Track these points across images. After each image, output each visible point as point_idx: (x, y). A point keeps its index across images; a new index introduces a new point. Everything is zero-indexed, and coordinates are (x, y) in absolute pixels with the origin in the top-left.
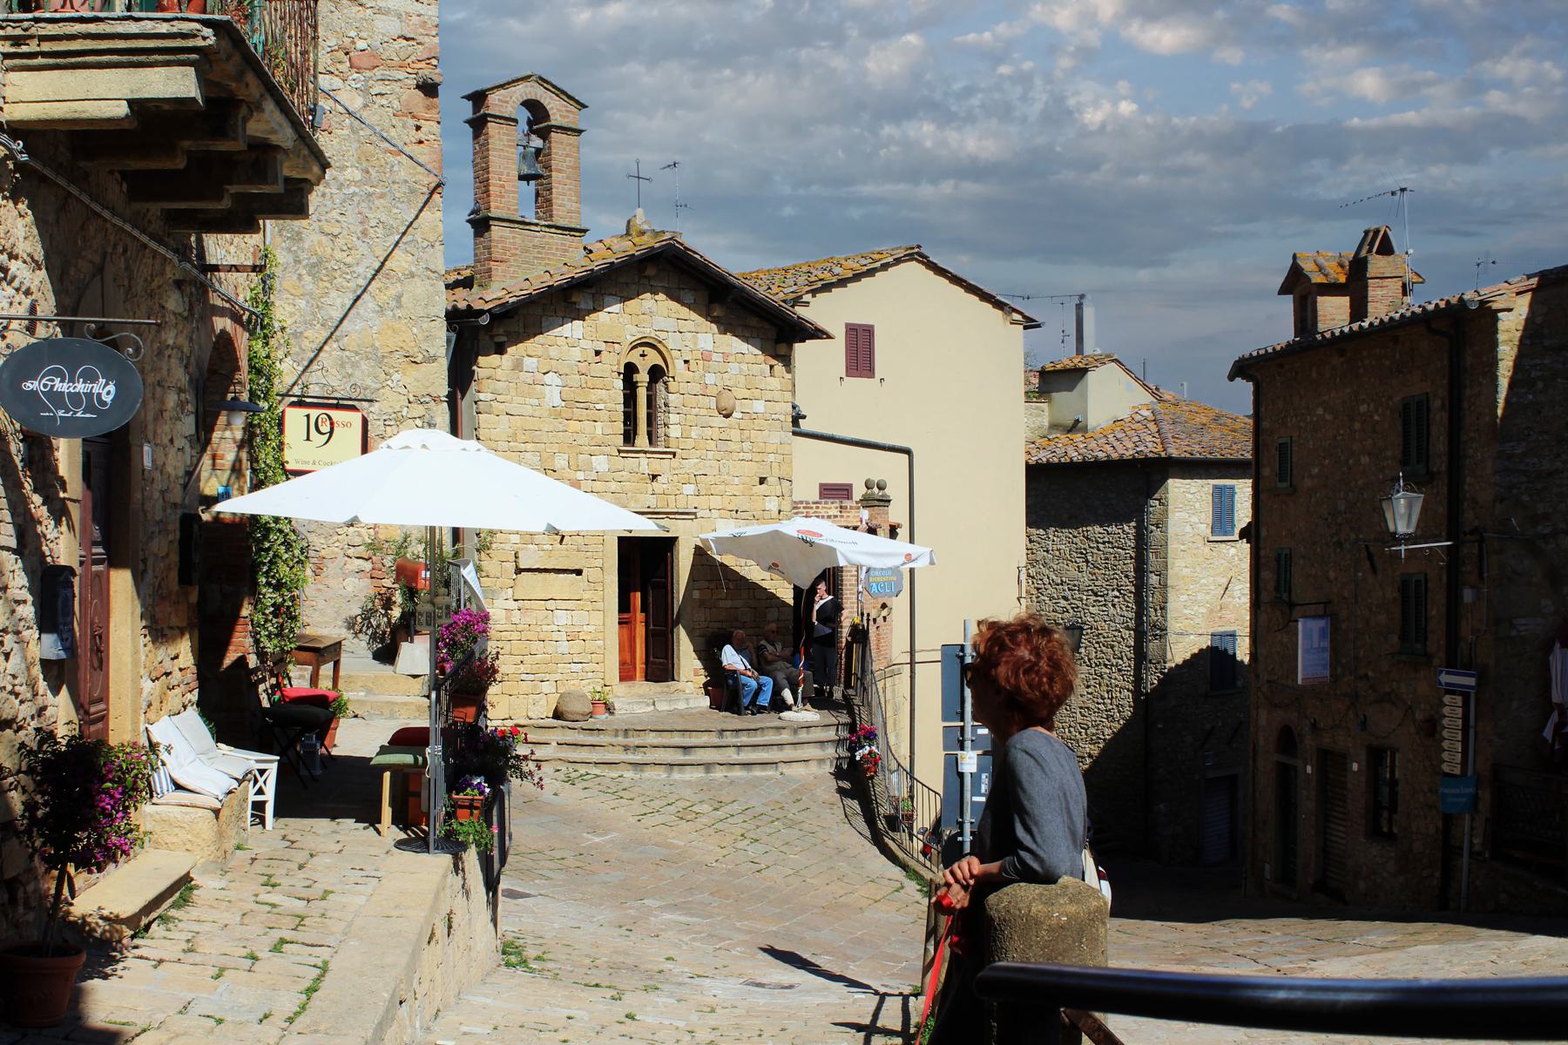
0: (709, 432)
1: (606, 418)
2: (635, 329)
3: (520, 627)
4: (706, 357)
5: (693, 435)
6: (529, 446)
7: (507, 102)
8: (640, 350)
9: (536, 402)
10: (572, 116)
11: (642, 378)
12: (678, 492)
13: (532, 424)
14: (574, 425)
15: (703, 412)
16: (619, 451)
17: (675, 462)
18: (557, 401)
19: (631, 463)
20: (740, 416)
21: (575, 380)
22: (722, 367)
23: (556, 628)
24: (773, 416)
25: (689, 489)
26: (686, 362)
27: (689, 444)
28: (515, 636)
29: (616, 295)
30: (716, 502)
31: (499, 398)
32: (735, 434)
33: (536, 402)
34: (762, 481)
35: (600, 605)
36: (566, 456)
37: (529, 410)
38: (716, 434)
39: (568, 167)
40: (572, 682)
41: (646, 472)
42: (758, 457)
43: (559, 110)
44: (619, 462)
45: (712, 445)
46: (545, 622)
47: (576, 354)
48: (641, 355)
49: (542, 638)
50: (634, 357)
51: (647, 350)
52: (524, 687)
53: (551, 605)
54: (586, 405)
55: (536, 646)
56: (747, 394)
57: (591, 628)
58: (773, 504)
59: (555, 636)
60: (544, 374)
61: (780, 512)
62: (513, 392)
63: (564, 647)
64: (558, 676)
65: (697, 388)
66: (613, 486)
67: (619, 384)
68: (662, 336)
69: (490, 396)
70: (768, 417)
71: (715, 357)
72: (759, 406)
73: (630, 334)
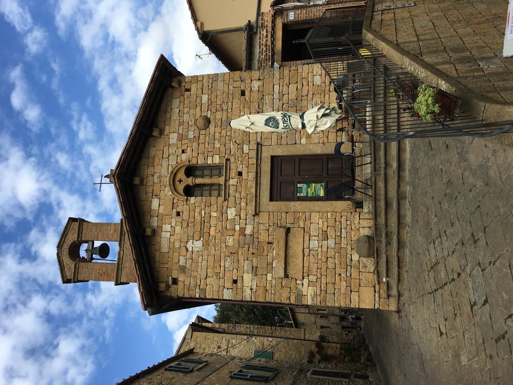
3: (319, 276)
4: (181, 137)
6: (222, 264)
7: (70, 267)
8: (177, 183)
9: (201, 257)
12: (247, 157)
13: (211, 259)
14: (212, 233)
16: (225, 200)
17: (232, 159)
20: (209, 112)
21: (190, 230)
23: (320, 249)
24: (210, 87)
25: (246, 148)
29: (151, 201)
31: (198, 284)
32: (219, 115)
33: (201, 257)
34: (243, 93)
36: (228, 237)
37: (204, 263)
38: (218, 130)
39: (96, 231)
40: (353, 236)
42: (231, 97)
45: (223, 132)
46: (316, 257)
47: (178, 229)
48: (180, 183)
49: (324, 260)
50: (181, 187)
51: (178, 179)
52: (355, 274)
53: (307, 251)
56: (199, 108)
57: (321, 223)
59: (324, 249)
61: (259, 79)
62: (196, 274)
63: (331, 242)
64: (349, 248)
65: (195, 145)
66: (243, 204)
68: (170, 169)
69: (198, 290)
70: (210, 91)
72: (205, 98)
73: (168, 192)
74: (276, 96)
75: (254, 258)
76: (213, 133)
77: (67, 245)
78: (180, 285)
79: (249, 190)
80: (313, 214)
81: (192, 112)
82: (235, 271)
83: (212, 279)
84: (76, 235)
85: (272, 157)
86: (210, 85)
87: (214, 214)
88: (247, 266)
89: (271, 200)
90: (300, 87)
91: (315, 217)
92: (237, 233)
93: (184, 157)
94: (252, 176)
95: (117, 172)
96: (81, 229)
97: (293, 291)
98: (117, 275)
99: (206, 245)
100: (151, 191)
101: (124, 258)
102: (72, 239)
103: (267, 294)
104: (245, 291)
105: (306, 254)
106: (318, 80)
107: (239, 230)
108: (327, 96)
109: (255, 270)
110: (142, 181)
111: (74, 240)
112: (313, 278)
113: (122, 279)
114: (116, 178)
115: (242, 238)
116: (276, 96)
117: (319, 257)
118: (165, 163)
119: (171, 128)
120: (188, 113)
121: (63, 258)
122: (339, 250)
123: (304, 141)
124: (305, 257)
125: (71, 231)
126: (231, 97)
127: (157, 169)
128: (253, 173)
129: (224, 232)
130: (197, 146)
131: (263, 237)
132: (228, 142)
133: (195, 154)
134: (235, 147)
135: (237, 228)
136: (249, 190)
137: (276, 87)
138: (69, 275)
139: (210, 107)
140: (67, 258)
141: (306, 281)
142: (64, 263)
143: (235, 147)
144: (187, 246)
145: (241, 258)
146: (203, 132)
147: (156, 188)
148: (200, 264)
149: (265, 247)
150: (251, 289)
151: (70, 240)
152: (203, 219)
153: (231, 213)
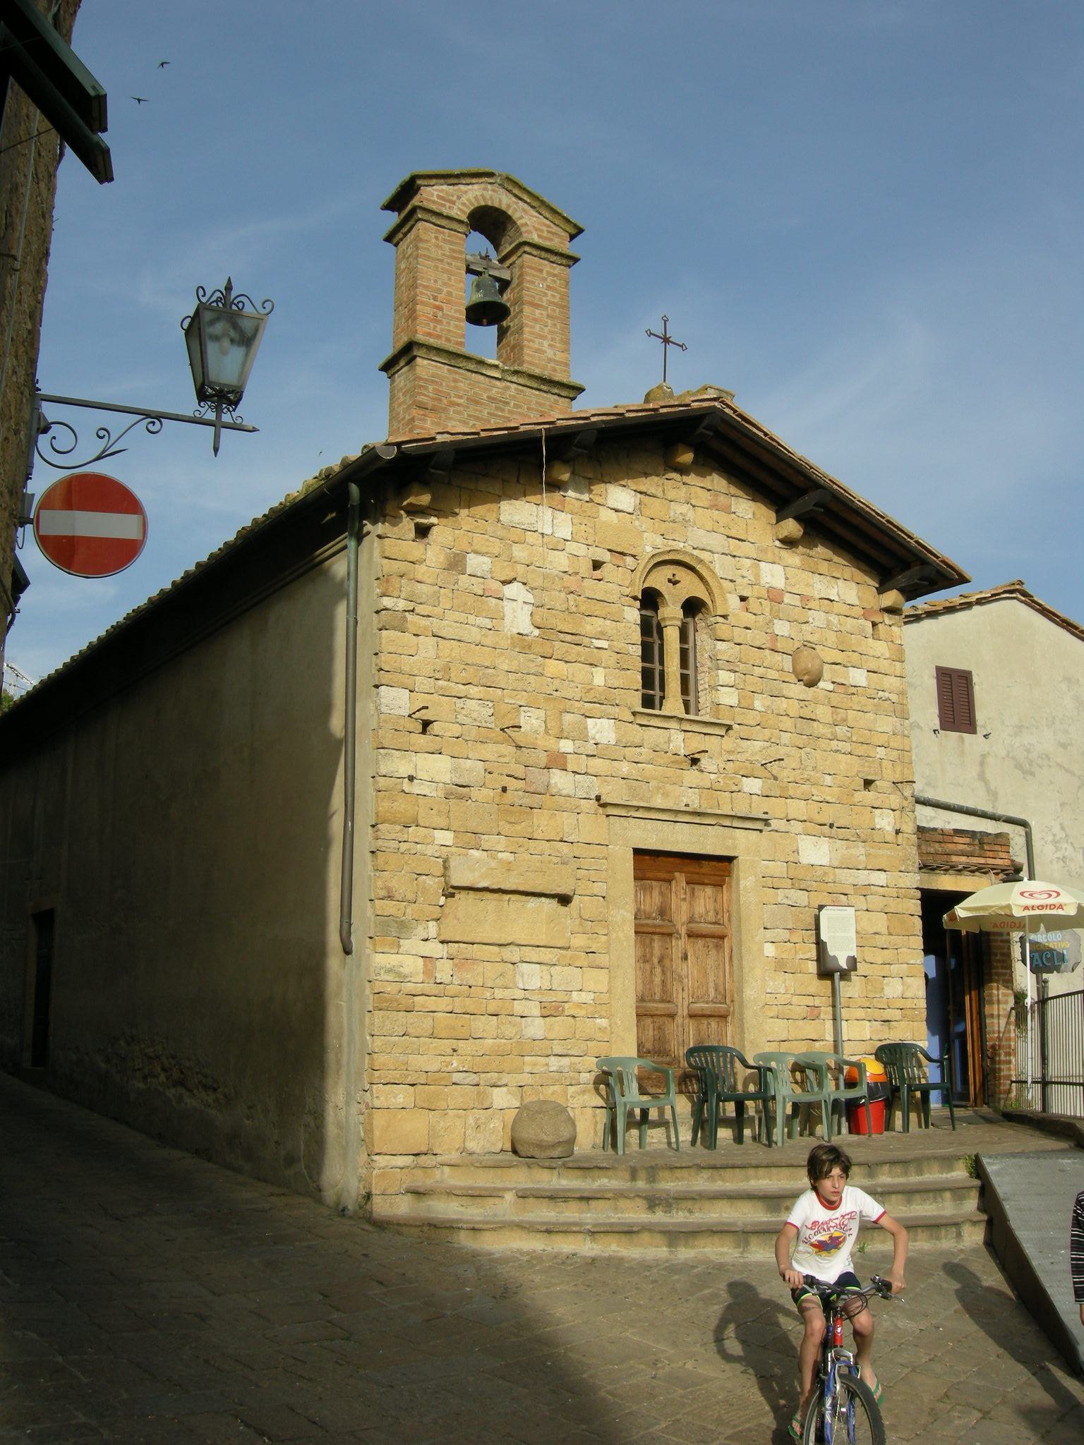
0: (783, 704)
1: (612, 662)
2: (659, 541)
3: (452, 989)
4: (774, 596)
5: (759, 703)
6: (473, 691)
7: (453, 203)
8: (668, 571)
10: (557, 240)
11: (671, 612)
12: (734, 788)
13: (485, 657)
14: (553, 667)
15: (772, 674)
16: (634, 714)
17: (728, 742)
18: (525, 625)
19: (653, 736)
20: (831, 687)
21: (557, 599)
22: (797, 613)
23: (520, 994)
25: (753, 785)
26: (743, 599)
27: (751, 718)
28: (444, 1004)
30: (797, 808)
31: (419, 609)
32: (823, 712)
34: (868, 783)
35: (602, 959)
37: (475, 635)
38: (794, 708)
39: (551, 303)
41: (682, 752)
42: (861, 750)
43: (536, 230)
44: (636, 733)
45: (787, 723)
46: (499, 982)
47: (560, 561)
48: (670, 581)
50: (658, 581)
51: (681, 573)
52: (456, 1096)
53: (513, 954)
54: (576, 638)
55: (482, 1025)
56: (838, 657)
57: (586, 997)
58: (886, 820)
59: (518, 1008)
60: (504, 583)
61: (898, 832)
63: (536, 1027)
64: (525, 1079)
65: (761, 639)
66: (625, 768)
67: (633, 614)
68: (705, 556)
69: (402, 605)
70: (872, 693)
71: (787, 598)
72: (858, 677)
73: (650, 544)
74: (863, 877)
75: (491, 793)
76: (785, 693)
77: (509, 206)
78: (415, 549)
79: (659, 788)
80: (603, 976)
81: (832, 638)
82: (456, 730)
83: (432, 653)
84: (535, 239)
85: (730, 859)
86: (886, 695)
87: (599, 677)
88: (472, 769)
89: (637, 852)
90: (882, 941)
91: (598, 980)
92: (550, 743)
93: (734, 601)
94: (693, 800)
95: (727, 410)
96: (554, 258)
97: (409, 911)
98: (439, 351)
99: (521, 643)
100: (652, 490)
101: (482, 378)
102: (526, 224)
103: (398, 828)
104: (403, 757)
105: (507, 953)
106: (893, 989)
107: (562, 750)
108: (860, 1013)
109: (459, 791)
110: (682, 470)
111: (523, 229)
112: (444, 971)
113: (426, 362)
114: (712, 404)
115: (543, 759)
116: (863, 877)
117: (499, 993)
118: (717, 541)
119: (796, 570)
120: (829, 625)
121: (476, 187)
122: (523, 1049)
123: (770, 950)
124: (496, 949)
125: (546, 225)
126: (861, 750)
127: (705, 517)
128: (697, 801)
129: (555, 701)
130: (758, 644)
131: (543, 823)
132: (767, 733)
133: (739, 635)
134: (756, 754)
135: (566, 746)
136: (659, 788)
137: (880, 878)
138: (431, 195)
139: (841, 689)
140: (476, 198)
141: (435, 949)
142: (462, 187)
143: (756, 754)
144: (515, 584)
145: (489, 751)
146: (787, 663)
147: (655, 506)
148: (471, 619)
149: (518, 827)
150: (411, 778)
151: (522, 218)
152: (586, 641)
153: (603, 730)
